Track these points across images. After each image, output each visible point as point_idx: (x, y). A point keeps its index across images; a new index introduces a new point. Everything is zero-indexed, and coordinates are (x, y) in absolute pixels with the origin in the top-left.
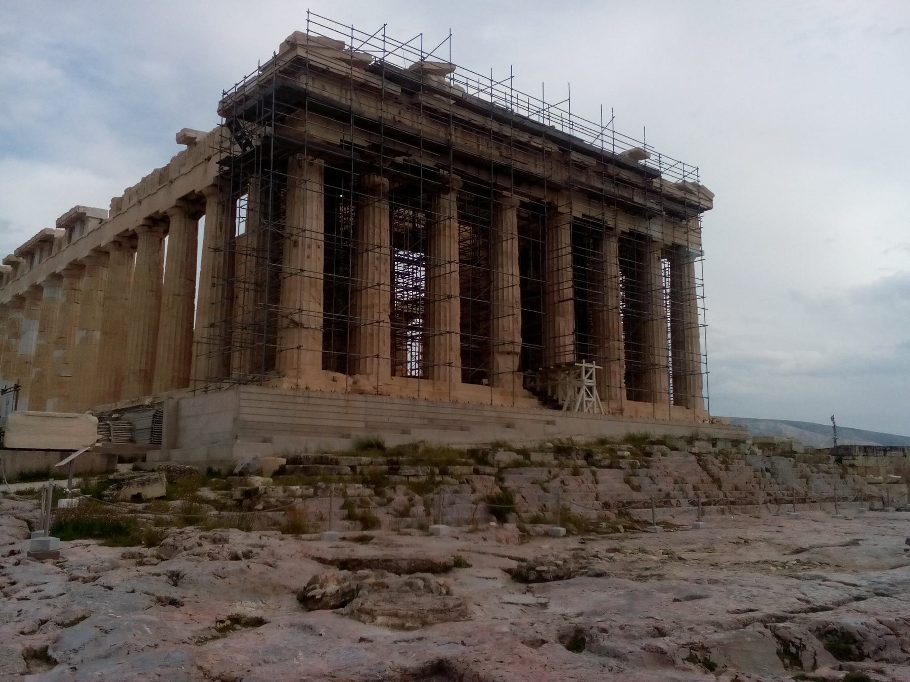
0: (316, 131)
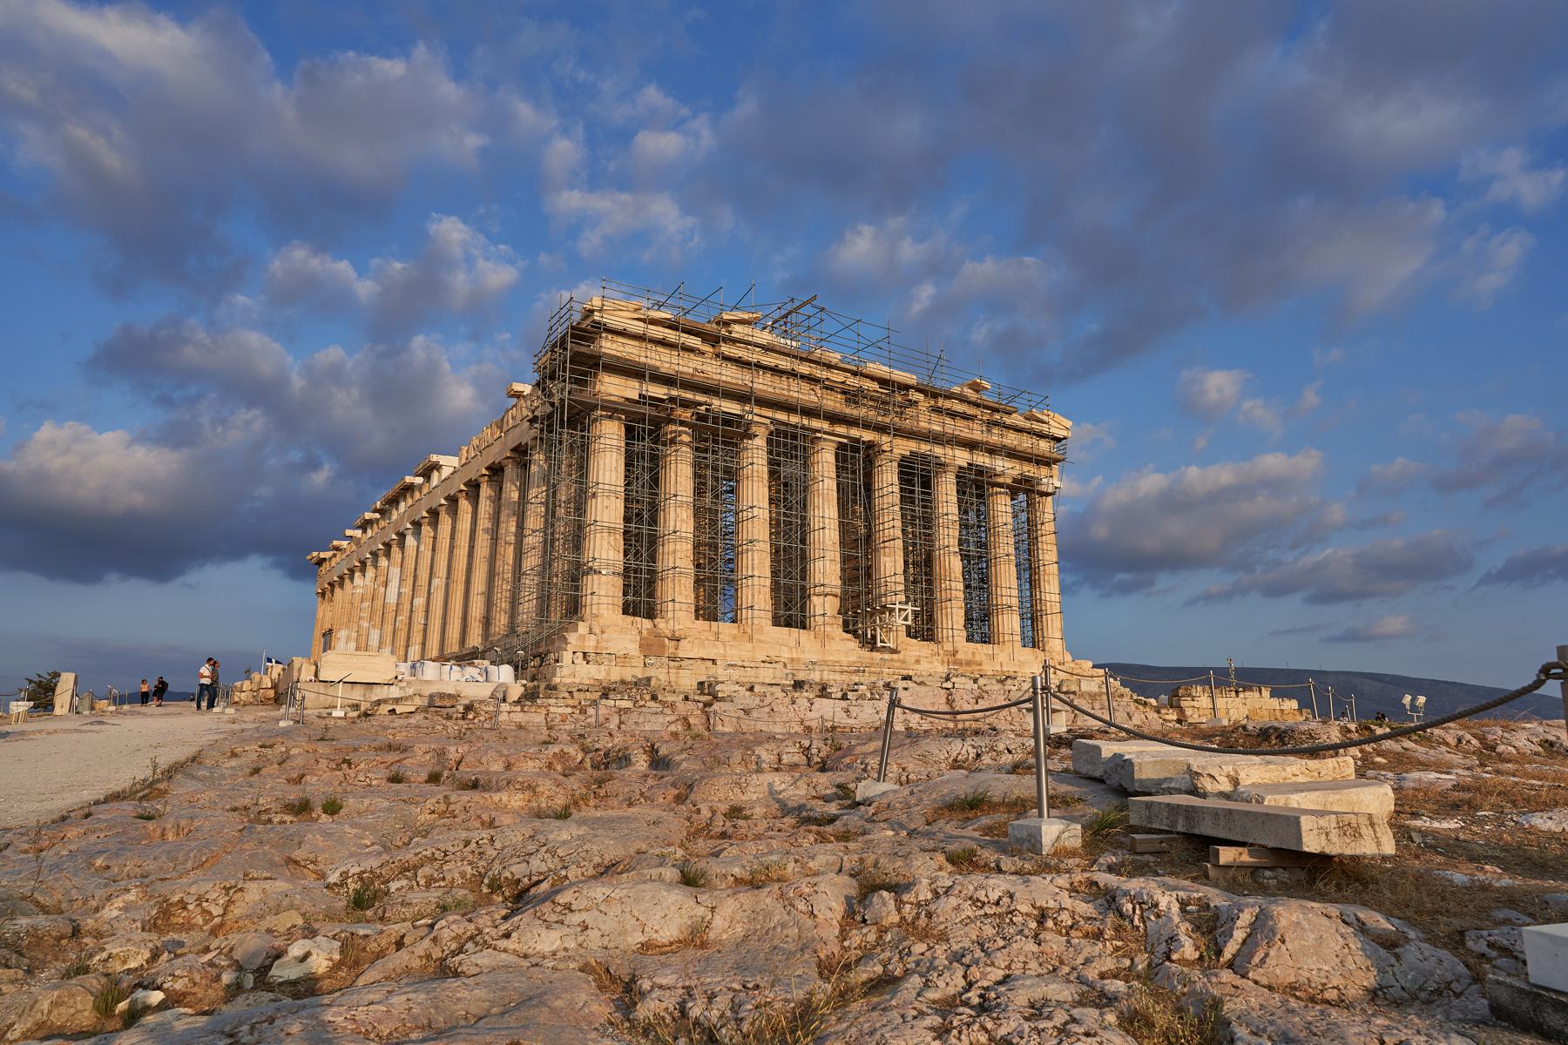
0: (613, 387)
